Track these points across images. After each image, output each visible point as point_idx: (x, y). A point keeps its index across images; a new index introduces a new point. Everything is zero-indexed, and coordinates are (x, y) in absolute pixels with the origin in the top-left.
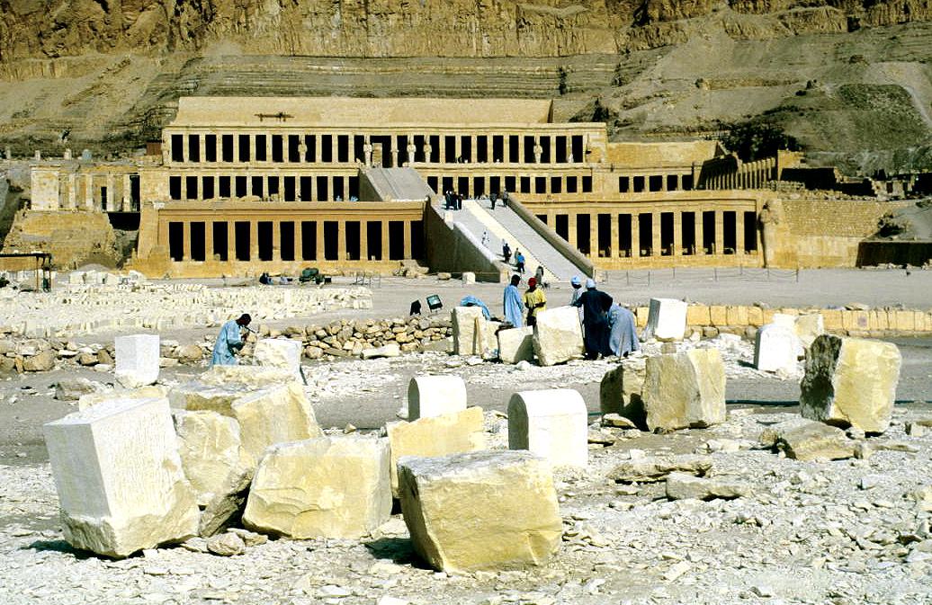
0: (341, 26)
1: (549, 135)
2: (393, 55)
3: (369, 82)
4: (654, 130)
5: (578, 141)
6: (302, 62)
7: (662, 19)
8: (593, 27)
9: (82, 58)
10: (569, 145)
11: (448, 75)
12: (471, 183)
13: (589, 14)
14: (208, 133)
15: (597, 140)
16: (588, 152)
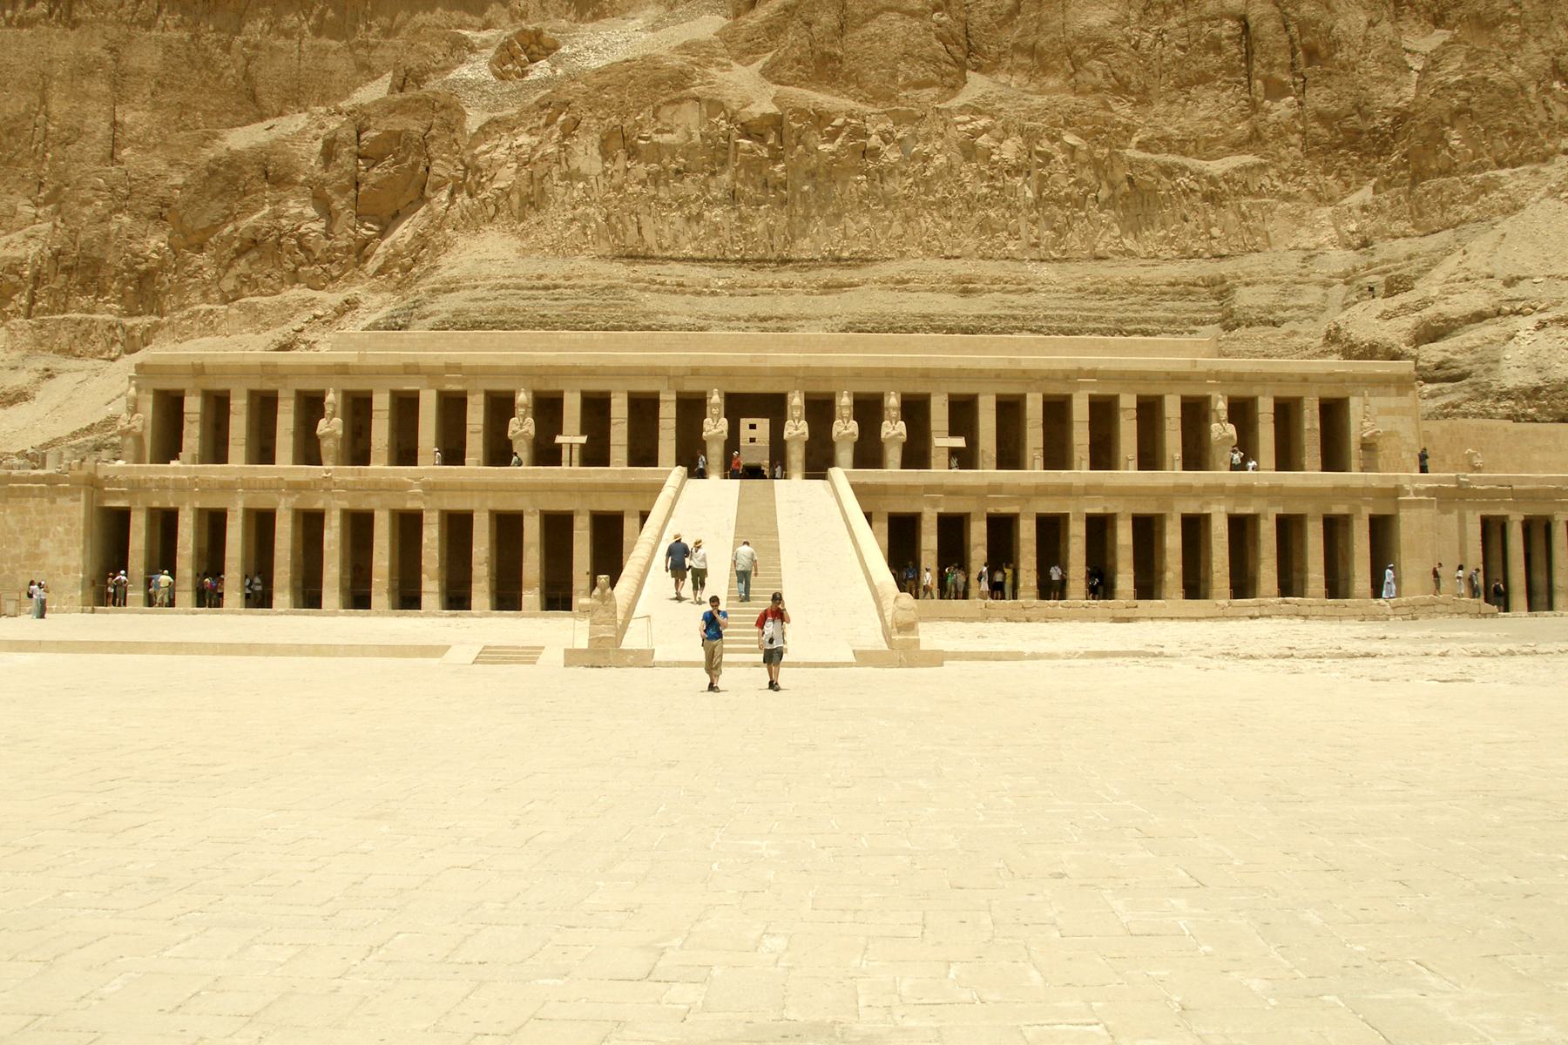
0: (733, 197)
1: (1255, 391)
2: (846, 254)
3: (786, 305)
4: (1537, 390)
5: (1333, 412)
6: (644, 270)
7: (1446, 172)
8: (1288, 197)
9: (279, 297)
10: (1311, 421)
11: (966, 288)
12: (1027, 533)
13: (1272, 172)
14: (256, 386)
15: (1390, 412)
16: (1368, 446)
